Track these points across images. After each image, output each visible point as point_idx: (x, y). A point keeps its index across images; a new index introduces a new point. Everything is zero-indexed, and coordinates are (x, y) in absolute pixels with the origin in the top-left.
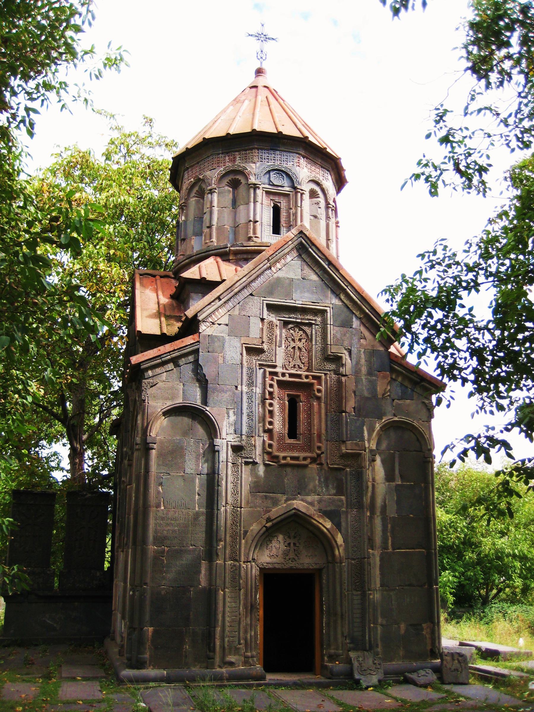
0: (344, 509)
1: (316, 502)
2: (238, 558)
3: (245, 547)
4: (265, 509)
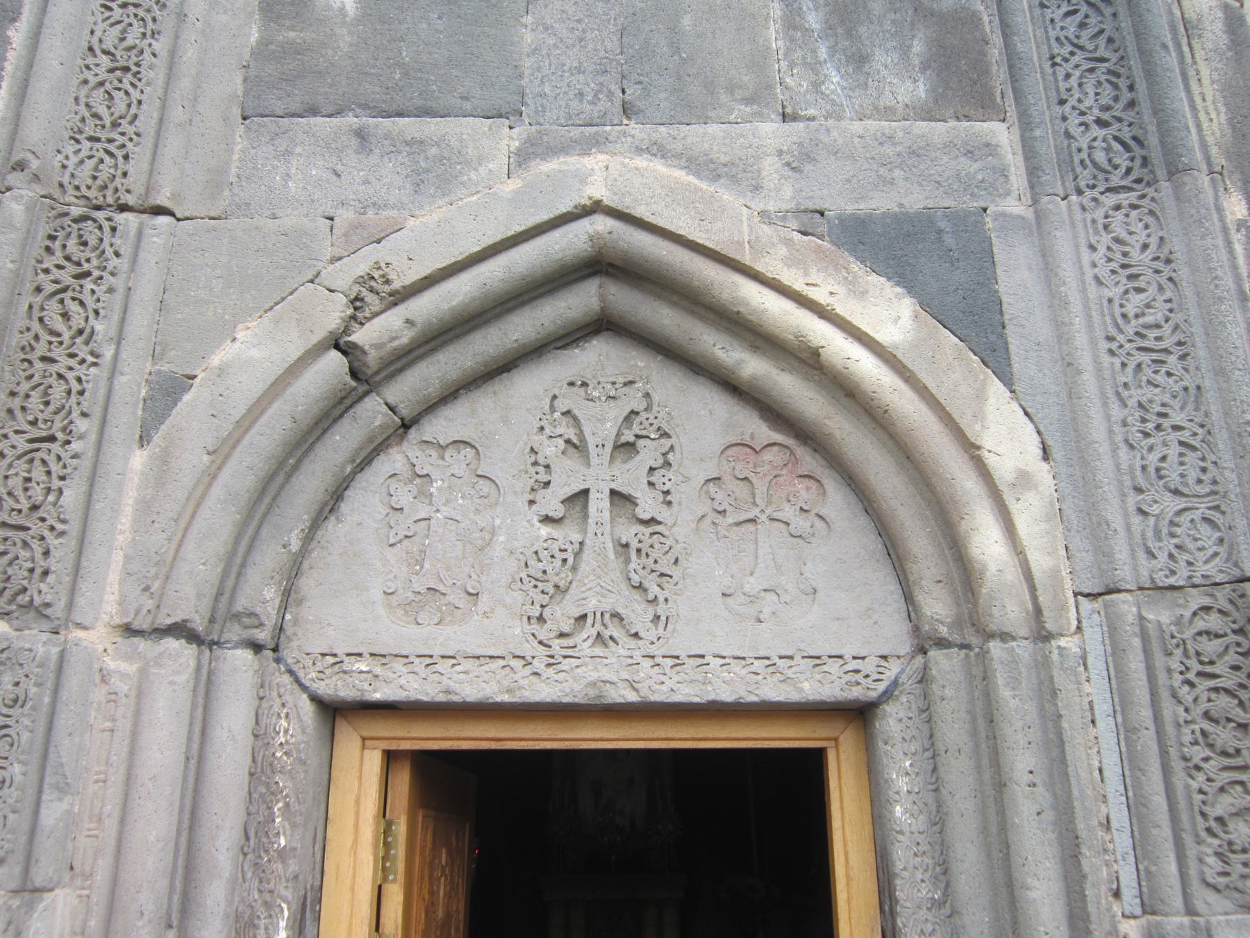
1: (770, 167)
2: (49, 591)
3: (146, 507)
4: (345, 216)
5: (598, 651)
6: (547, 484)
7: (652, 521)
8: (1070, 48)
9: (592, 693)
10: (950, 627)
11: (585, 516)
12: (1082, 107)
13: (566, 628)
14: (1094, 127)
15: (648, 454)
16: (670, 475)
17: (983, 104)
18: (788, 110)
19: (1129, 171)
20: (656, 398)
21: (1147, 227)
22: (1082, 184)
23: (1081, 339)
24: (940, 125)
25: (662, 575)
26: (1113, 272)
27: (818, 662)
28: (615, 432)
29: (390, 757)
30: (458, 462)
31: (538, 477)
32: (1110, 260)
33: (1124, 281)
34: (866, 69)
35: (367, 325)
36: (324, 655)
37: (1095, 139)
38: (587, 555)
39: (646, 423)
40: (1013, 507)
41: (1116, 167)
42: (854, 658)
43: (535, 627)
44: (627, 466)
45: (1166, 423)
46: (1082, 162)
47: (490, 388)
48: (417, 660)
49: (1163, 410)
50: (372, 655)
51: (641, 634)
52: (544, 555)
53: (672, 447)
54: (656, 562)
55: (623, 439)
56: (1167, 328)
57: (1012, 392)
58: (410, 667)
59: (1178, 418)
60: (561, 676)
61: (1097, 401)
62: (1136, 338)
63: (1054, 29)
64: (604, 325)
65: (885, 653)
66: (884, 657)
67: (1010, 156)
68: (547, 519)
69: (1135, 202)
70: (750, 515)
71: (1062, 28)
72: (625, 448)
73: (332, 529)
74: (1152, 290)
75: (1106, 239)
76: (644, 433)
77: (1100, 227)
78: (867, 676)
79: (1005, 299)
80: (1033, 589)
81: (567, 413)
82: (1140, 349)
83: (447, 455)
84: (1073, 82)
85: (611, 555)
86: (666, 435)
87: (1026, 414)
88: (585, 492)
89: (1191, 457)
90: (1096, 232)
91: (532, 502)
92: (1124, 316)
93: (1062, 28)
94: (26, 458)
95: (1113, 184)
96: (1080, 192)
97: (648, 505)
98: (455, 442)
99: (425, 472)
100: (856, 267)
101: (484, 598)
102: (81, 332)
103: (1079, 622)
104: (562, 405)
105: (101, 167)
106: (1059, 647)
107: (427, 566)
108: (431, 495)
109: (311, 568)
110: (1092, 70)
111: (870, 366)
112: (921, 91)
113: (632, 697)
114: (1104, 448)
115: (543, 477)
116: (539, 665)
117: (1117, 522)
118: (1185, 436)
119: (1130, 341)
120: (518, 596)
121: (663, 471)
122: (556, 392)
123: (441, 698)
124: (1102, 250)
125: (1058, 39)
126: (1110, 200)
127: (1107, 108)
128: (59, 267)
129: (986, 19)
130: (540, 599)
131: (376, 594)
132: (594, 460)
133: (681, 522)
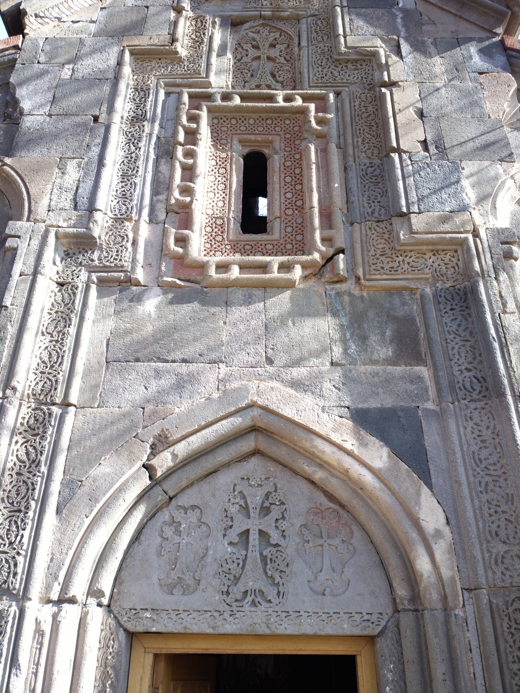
0: (430, 405)
5: (253, 609)
6: (231, 527)
7: (277, 545)
8: (453, 335)
9: (250, 629)
10: (409, 601)
11: (248, 542)
12: (460, 363)
13: (239, 597)
14: (465, 371)
15: (275, 513)
16: (285, 523)
17: (418, 359)
18: (334, 361)
19: (480, 392)
20: (279, 486)
21: (488, 418)
22: (460, 397)
23: (461, 469)
24: (398, 368)
25: (281, 571)
26: (474, 438)
27: (351, 615)
28: (261, 501)
29: (156, 656)
30: (193, 517)
31: (227, 523)
32: (473, 433)
33: (479, 443)
34: (367, 343)
35: (157, 457)
36: (131, 609)
37: (465, 377)
38: (249, 561)
39: (275, 498)
40: (435, 547)
41: (474, 390)
42: (367, 614)
43: (225, 597)
44: (266, 518)
45: (499, 509)
46: (460, 388)
47: (208, 480)
48: (172, 612)
49: (498, 503)
50: (152, 609)
51: (272, 600)
52: (229, 561)
53: (286, 509)
54: (278, 565)
55: (265, 505)
56: (499, 466)
57: (432, 492)
58: (169, 616)
59: (504, 508)
60: (237, 621)
61: (468, 498)
62: (485, 469)
63: (447, 327)
64: (256, 452)
65: (381, 612)
66: (381, 614)
67: (429, 382)
68: (231, 544)
69: (484, 406)
70: (321, 543)
71: (450, 327)
72: (265, 511)
73: (138, 548)
74: (491, 448)
75: (471, 424)
76: (273, 502)
77: (468, 418)
78: (373, 623)
79: (427, 448)
80: (443, 586)
81: (241, 492)
82: (486, 474)
83: (188, 513)
84: (455, 351)
85: (259, 561)
86: (283, 503)
87: (438, 502)
88: (248, 531)
89: (511, 526)
90: (467, 421)
91: (224, 535)
92: (480, 459)
93: (450, 327)
94: (8, 520)
95: (473, 398)
96: (459, 401)
97: (275, 537)
98: (192, 506)
99: (178, 520)
100: (363, 433)
101: (203, 582)
102: (34, 461)
103: (464, 602)
104: (238, 488)
105: (46, 385)
106: (455, 614)
107: (178, 566)
108: (181, 531)
109: (126, 567)
110: (463, 345)
111: (370, 478)
112: (390, 353)
113: (267, 632)
114: (472, 521)
115: (231, 524)
116: (226, 615)
117: (479, 557)
118: (507, 516)
119: (482, 471)
120: (218, 582)
121: (282, 521)
122: (236, 482)
123: (182, 631)
124: (469, 429)
125: (448, 332)
126: (473, 406)
127: (471, 363)
128: (25, 431)
129: (418, 319)
130: (227, 583)
131: (155, 580)
132: (252, 515)
133: (290, 547)
